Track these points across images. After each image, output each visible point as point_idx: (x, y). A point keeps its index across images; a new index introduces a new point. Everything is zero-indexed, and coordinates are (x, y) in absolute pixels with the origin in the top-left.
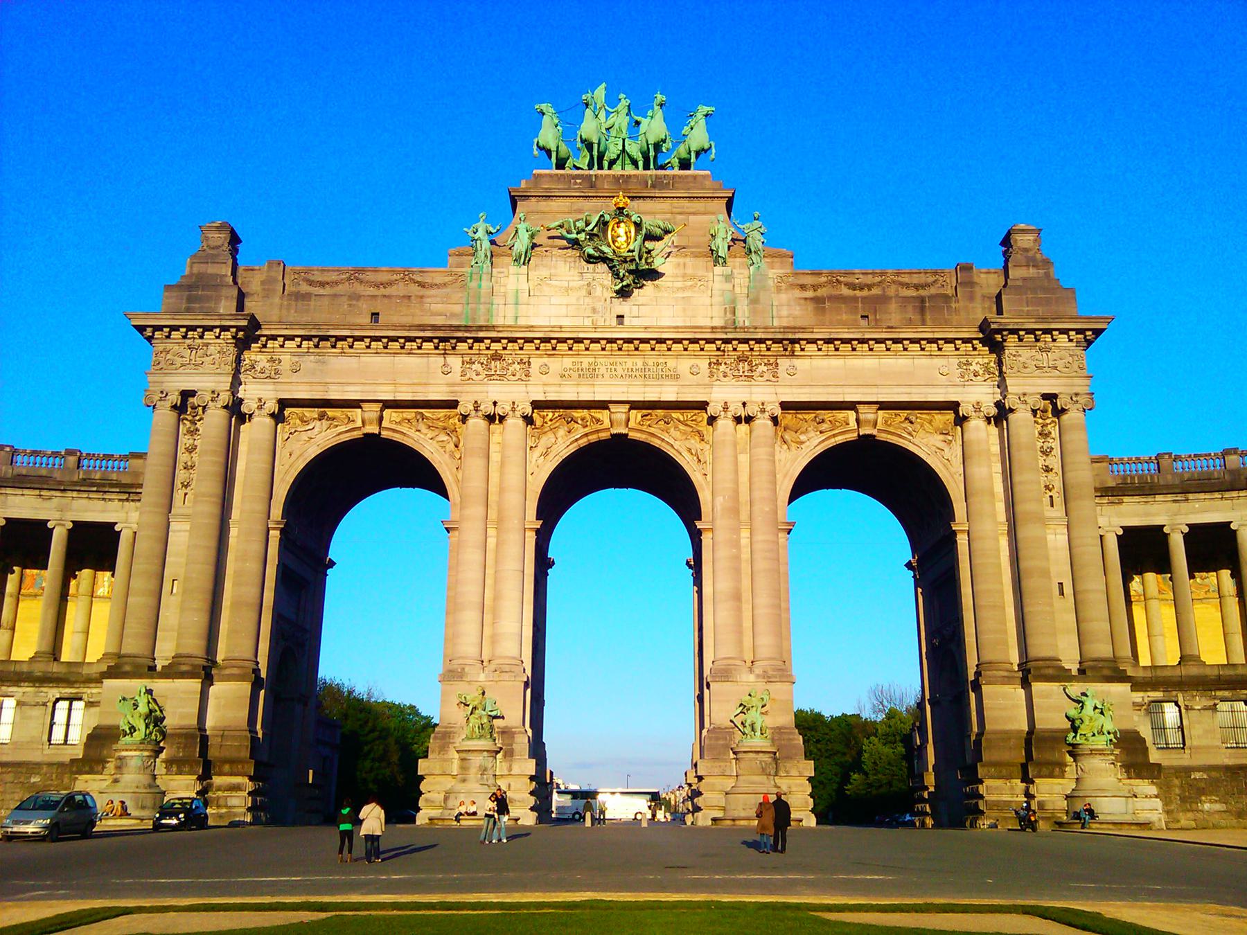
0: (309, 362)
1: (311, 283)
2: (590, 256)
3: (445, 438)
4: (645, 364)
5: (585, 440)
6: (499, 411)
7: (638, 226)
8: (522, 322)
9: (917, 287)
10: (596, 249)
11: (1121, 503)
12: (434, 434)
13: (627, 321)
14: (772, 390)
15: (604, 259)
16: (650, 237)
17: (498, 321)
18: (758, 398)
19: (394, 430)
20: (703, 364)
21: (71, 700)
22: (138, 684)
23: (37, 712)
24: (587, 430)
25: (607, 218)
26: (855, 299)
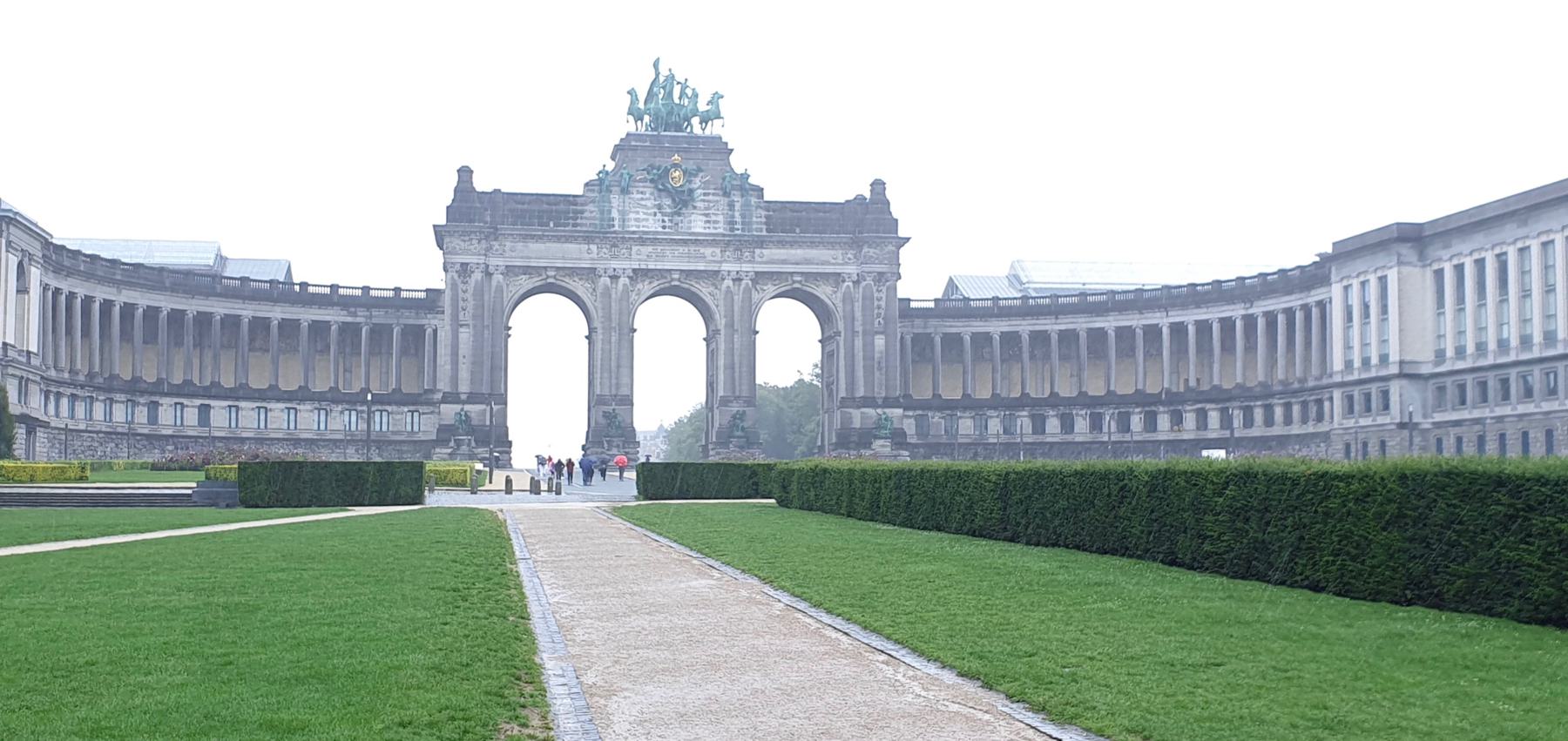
0: (520, 245)
1: (519, 203)
2: (660, 190)
7: (685, 172)
10: (663, 185)
18: (744, 269)
20: (718, 251)
21: (413, 412)
22: (458, 407)
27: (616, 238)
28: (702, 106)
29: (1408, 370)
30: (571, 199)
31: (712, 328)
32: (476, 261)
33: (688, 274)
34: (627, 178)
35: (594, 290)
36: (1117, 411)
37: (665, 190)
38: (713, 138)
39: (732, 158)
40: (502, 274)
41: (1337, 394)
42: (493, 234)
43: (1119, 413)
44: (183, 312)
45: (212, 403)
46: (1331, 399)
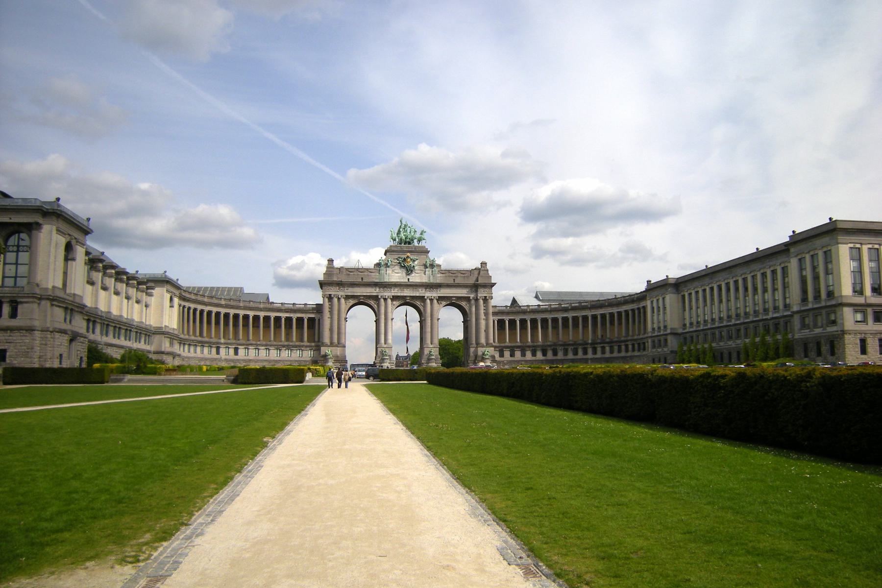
6: (386, 297)
8: (390, 280)
9: (464, 274)
15: (405, 266)
17: (385, 281)
23: (305, 352)
26: (452, 276)
28: (418, 235)
29: (673, 332)
30: (369, 270)
32: (334, 293)
33: (413, 297)
34: (390, 261)
38: (422, 247)
39: (429, 254)
40: (343, 298)
41: (650, 341)
42: (340, 284)
43: (574, 348)
44: (229, 313)
45: (239, 347)
46: (648, 342)
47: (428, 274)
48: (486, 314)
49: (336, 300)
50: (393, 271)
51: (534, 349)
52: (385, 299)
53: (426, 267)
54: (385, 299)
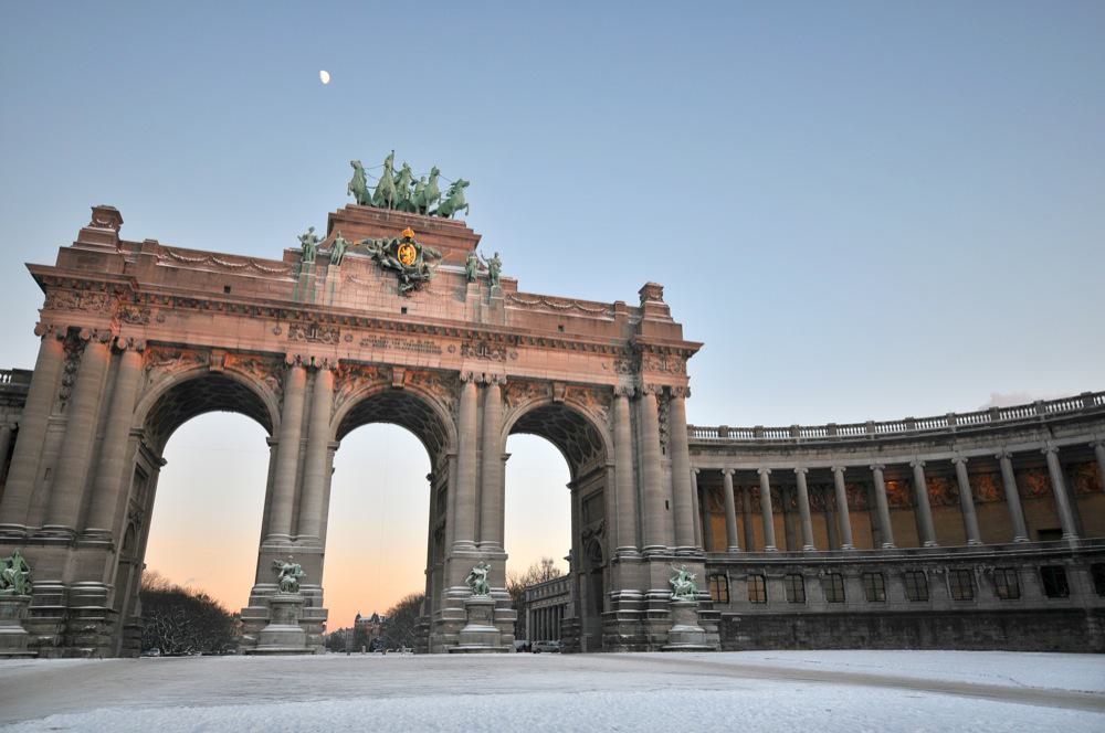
2: (385, 266)
3: (273, 379)
4: (419, 342)
5: (373, 389)
6: (317, 363)
7: (418, 251)
8: (336, 304)
10: (390, 261)
11: (699, 454)
12: (264, 376)
13: (409, 312)
14: (498, 367)
15: (393, 269)
16: (426, 259)
19: (234, 371)
20: (458, 345)
24: (375, 382)
25: (398, 243)
27: (319, 315)
31: (441, 457)
33: (417, 373)
34: (342, 247)
35: (280, 385)
36: (992, 568)
37: (393, 269)
40: (140, 351)
42: (128, 294)
47: (473, 300)
48: (669, 447)
49: (97, 353)
50: (349, 279)
51: (832, 574)
52: (312, 370)
53: (468, 278)
54: (312, 370)
